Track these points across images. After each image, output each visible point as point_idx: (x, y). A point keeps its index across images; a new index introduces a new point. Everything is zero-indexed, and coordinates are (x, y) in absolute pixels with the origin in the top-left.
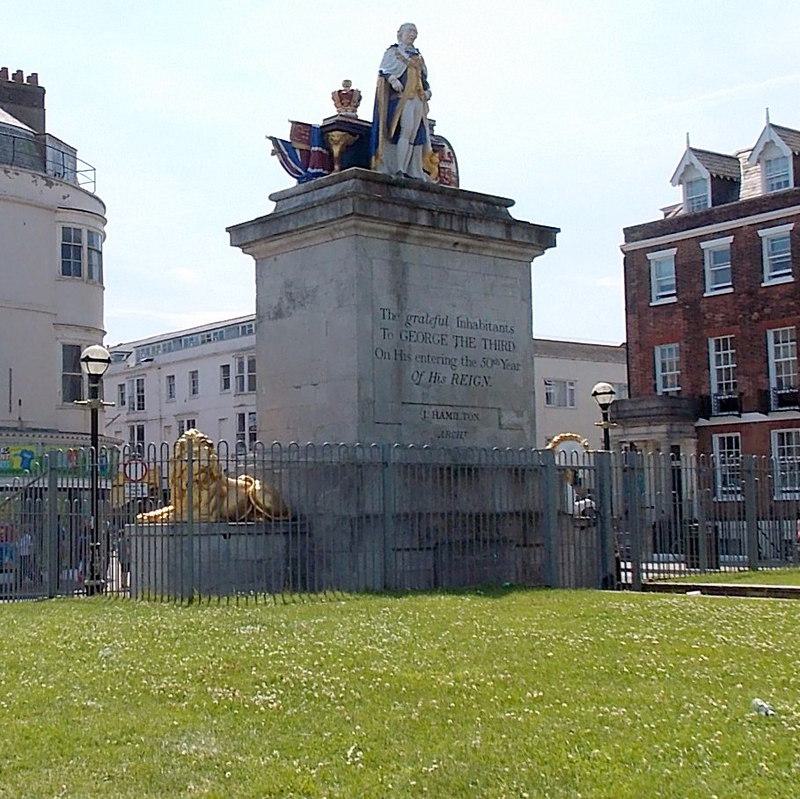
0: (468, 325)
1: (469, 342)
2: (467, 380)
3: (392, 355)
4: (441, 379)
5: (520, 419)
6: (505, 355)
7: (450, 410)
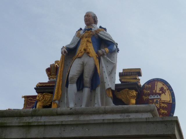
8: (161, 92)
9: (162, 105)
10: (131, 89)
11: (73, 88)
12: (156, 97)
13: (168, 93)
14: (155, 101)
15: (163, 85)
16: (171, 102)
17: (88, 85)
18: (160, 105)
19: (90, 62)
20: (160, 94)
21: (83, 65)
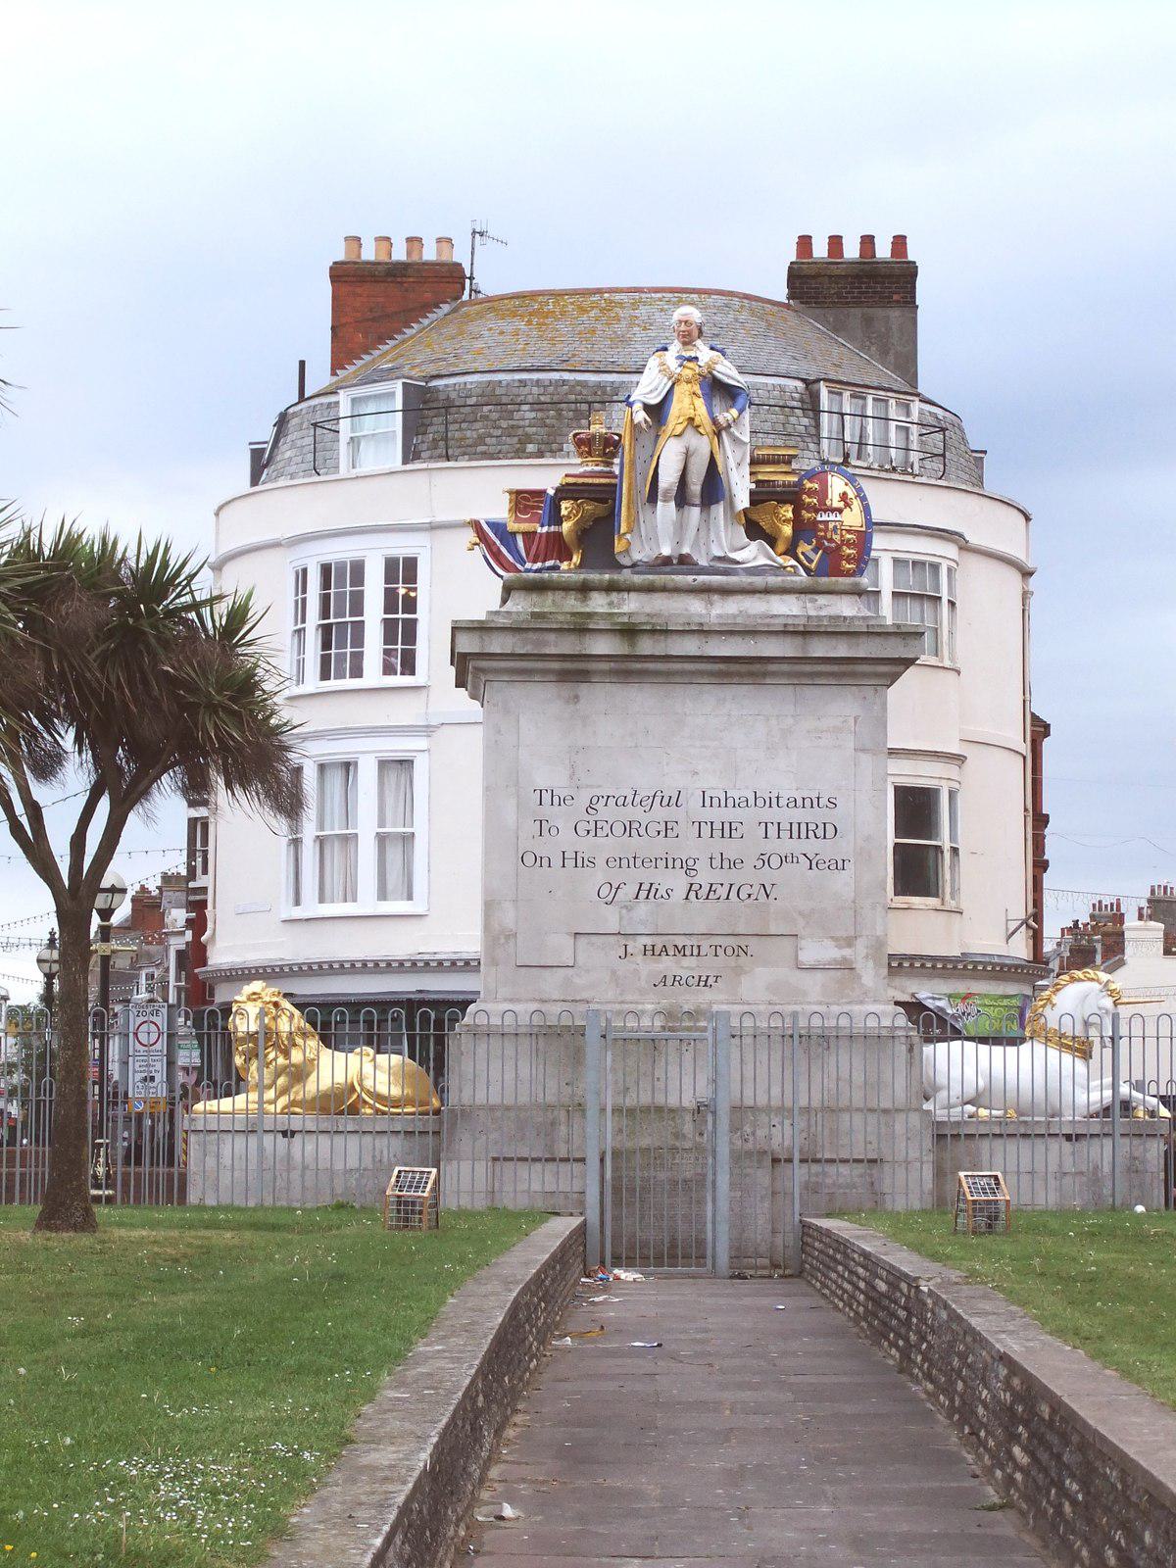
0: (726, 801)
1: (728, 830)
2: (722, 892)
3: (557, 862)
4: (662, 892)
5: (847, 952)
6: (811, 846)
7: (680, 942)
8: (842, 505)
9: (849, 536)
10: (783, 502)
11: (666, 510)
12: (832, 517)
13: (856, 504)
14: (831, 526)
15: (846, 484)
16: (863, 529)
17: (697, 501)
18: (842, 536)
19: (702, 446)
20: (840, 511)
21: (687, 455)
